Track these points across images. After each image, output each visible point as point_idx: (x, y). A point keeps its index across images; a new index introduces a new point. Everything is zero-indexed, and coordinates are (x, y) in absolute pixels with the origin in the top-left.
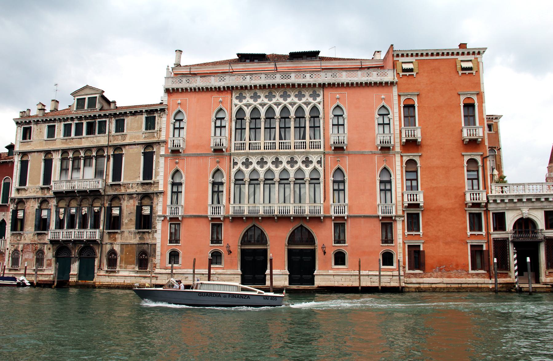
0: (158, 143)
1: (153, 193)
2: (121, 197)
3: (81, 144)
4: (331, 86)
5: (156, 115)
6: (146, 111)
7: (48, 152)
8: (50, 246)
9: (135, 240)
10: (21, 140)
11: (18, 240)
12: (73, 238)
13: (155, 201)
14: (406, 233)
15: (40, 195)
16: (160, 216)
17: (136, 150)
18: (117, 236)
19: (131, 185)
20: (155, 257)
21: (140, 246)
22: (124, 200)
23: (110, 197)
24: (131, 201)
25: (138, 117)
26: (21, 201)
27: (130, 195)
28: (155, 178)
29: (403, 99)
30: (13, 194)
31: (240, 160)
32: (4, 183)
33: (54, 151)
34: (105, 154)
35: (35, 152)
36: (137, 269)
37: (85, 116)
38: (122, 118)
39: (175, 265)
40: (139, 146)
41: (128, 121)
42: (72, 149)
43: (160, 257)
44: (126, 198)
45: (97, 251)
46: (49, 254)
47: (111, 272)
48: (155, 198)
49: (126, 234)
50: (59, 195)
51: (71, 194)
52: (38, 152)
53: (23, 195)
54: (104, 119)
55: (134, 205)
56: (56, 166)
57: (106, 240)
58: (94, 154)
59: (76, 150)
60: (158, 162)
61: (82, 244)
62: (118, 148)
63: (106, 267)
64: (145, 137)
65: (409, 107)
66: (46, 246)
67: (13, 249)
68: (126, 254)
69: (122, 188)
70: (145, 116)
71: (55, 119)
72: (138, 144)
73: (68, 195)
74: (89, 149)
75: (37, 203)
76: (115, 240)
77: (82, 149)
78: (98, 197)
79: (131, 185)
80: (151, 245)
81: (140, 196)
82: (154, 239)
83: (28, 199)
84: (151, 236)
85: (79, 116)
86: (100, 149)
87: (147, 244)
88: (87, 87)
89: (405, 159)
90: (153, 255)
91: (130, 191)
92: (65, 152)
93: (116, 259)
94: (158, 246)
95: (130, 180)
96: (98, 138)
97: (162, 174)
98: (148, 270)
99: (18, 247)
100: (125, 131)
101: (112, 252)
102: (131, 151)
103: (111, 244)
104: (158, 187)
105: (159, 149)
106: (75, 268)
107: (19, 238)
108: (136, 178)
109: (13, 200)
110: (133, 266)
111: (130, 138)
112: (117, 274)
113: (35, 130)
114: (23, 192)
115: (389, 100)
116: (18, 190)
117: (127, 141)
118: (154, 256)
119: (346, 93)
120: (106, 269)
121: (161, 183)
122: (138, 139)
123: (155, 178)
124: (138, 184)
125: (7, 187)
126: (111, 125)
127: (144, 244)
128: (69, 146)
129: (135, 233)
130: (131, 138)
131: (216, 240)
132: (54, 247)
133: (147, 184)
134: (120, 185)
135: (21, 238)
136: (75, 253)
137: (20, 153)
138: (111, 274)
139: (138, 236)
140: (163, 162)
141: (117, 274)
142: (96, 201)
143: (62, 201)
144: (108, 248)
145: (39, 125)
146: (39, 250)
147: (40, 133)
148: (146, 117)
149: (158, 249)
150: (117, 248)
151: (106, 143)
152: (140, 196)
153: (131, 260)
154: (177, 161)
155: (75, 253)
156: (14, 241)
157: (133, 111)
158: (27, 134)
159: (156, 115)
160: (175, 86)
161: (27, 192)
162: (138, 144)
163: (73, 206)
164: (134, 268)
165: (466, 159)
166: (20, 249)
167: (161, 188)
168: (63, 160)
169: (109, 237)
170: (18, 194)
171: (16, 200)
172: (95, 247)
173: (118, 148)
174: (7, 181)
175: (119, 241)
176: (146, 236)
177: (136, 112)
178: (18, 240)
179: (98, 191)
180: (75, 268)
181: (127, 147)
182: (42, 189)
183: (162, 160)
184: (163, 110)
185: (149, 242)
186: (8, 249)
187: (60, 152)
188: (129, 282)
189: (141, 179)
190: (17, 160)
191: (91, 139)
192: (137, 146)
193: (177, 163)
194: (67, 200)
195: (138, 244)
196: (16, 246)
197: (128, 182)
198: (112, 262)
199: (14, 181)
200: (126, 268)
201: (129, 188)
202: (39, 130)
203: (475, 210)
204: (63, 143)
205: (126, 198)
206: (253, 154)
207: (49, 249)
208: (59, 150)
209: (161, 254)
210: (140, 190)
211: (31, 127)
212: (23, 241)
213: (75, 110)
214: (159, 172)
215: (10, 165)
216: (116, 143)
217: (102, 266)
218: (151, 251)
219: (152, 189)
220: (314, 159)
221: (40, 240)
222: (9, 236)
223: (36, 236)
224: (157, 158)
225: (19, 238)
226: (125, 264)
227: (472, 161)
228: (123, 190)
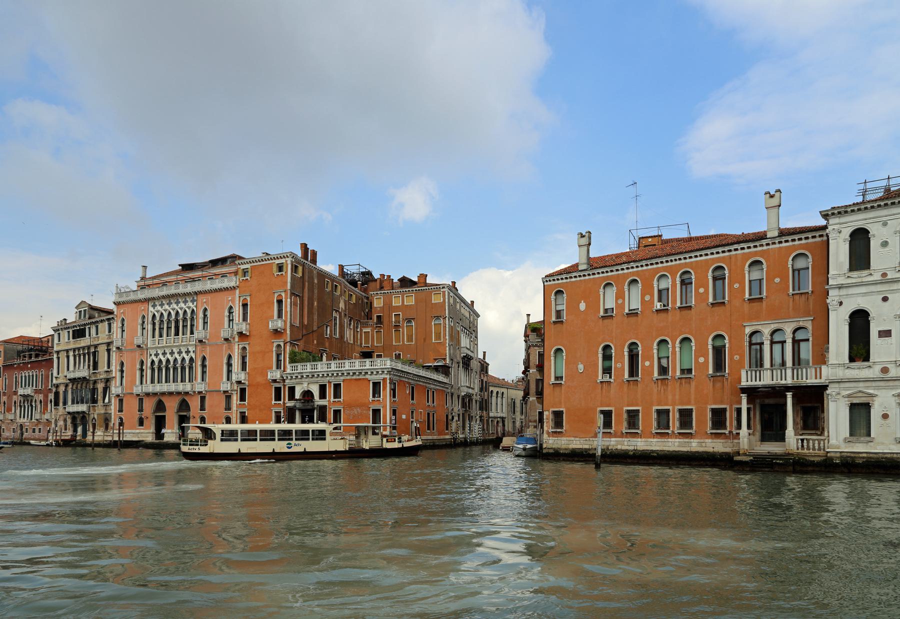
4: (200, 292)
7: (67, 351)
9: (103, 412)
14: (239, 402)
26: (57, 386)
29: (242, 299)
31: (153, 352)
46: (69, 421)
57: (92, 411)
59: (79, 349)
65: (245, 306)
74: (83, 348)
89: (241, 346)
91: (102, 377)
92: (74, 350)
106: (80, 429)
115: (233, 301)
117: (100, 342)
119: (209, 297)
131: (141, 410)
160: (120, 300)
165: (275, 345)
168: (75, 356)
173: (96, 346)
179: (84, 378)
180: (80, 429)
190: (55, 356)
203: (277, 385)
206: (159, 348)
216: (96, 343)
220: (191, 349)
227: (279, 346)
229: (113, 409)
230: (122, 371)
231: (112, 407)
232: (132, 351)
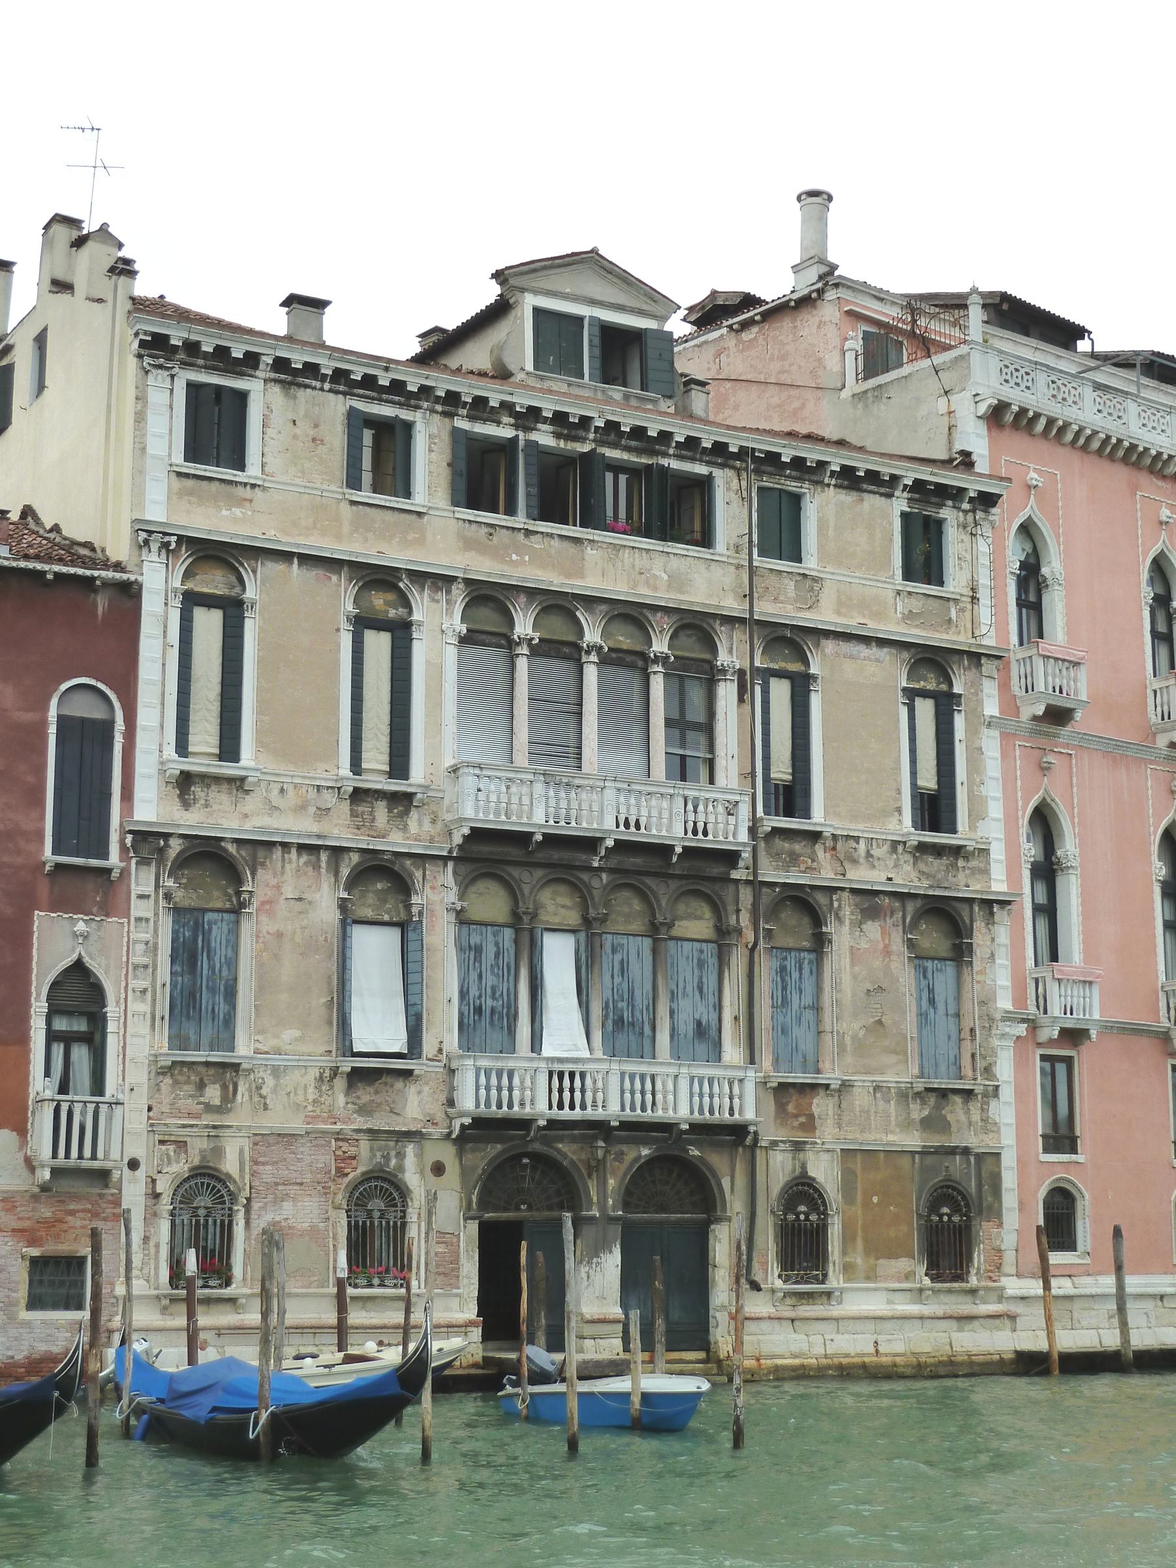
0: (975, 658)
1: (970, 901)
2: (821, 899)
3: (580, 574)
5: (947, 513)
6: (919, 486)
7: (377, 577)
8: (447, 1154)
10: (178, 457)
11: (209, 1108)
12: (614, 1108)
13: (980, 938)
15: (340, 830)
16: (1008, 1017)
17: (871, 668)
18: (820, 1105)
19: (862, 846)
20: (999, 1215)
21: (929, 1160)
22: (839, 919)
23: (767, 896)
24: (873, 929)
25: (872, 502)
27: (870, 901)
28: (972, 827)
30: (151, 805)
32: (61, 719)
33: (420, 577)
34: (723, 658)
35: (285, 556)
36: (927, 1281)
37: (612, 426)
38: (792, 486)
39: (1056, 1258)
40: (884, 653)
41: (821, 508)
42: (532, 593)
43: (1013, 1224)
44: (847, 912)
45: (726, 1183)
47: (809, 1296)
48: (979, 925)
49: (860, 1098)
50: (491, 853)
51: (556, 855)
52: (307, 560)
53: (221, 818)
54: (701, 469)
55: (887, 952)
56: (435, 671)
58: (660, 646)
60: (976, 753)
61: (645, 1142)
62: (783, 640)
63: (776, 1274)
64: (910, 616)
66: (410, 1149)
67: (180, 1168)
68: (867, 1204)
69: (819, 848)
70: (900, 504)
71: (425, 391)
72: (882, 642)
73: (540, 856)
74: (631, 614)
75: (327, 881)
76: (810, 1125)
77: (590, 601)
78: (705, 888)
79: (862, 846)
80: (980, 1157)
81: (911, 907)
82: (989, 1125)
83: (260, 847)
84: (975, 1107)
85: (575, 411)
86: (696, 626)
87: (966, 1151)
88: (590, 261)
90: (990, 1208)
92: (488, 598)
93: (825, 1227)
94: (1009, 1161)
95: (854, 817)
96: (674, 563)
97: (995, 810)
98: (973, 1281)
99: (218, 1152)
100: (811, 562)
101: (802, 1191)
102: (849, 667)
103: (798, 1147)
104: (986, 872)
105: (976, 687)
107: (213, 1094)
108: (884, 814)
109: (147, 842)
110: (903, 1264)
111: (840, 603)
112: (835, 1311)
113: (277, 420)
114: (220, 798)
116: (185, 782)
117: (825, 616)
118: (995, 1213)
120: (779, 1283)
121: (998, 852)
122: (879, 615)
123: (972, 827)
124: (894, 844)
125: (90, 752)
126: (732, 509)
127: (953, 1151)
128: (508, 570)
129: (905, 1096)
130: (842, 605)
132: (469, 1158)
133: (938, 851)
134: (815, 836)
135: (229, 1097)
136: (605, 1193)
137: (180, 538)
138: (806, 1310)
139: (918, 1111)
140: (998, 755)
141: (835, 1311)
142: (681, 908)
143: (481, 885)
144: (778, 1168)
145: (303, 395)
146: (367, 1177)
147: (291, 446)
148: (904, 515)
149: (1009, 1180)
150: (824, 1171)
151: (733, 606)
152: (911, 907)
153: (892, 1234)
154: (1050, 758)
155: (605, 1193)
156: (176, 1112)
157: (862, 465)
158: (215, 431)
159: (947, 513)
161: (251, 803)
162: (882, 642)
163: (555, 920)
164: (909, 1276)
166: (230, 1165)
167: (999, 885)
169: (781, 1108)
170: (186, 805)
171: (176, 846)
172: (718, 1161)
173: (789, 641)
174: (86, 709)
175: (828, 1134)
176: (956, 1111)
177: (873, 477)
178: (209, 1108)
181: (829, 646)
182: (359, 795)
183: (991, 743)
184: (987, 500)
185: (974, 1141)
186: (133, 1165)
187: (459, 594)
188: (899, 1347)
189: (904, 825)
191: (640, 561)
192: (874, 651)
193: (1045, 769)
194: (527, 879)
195: (925, 1152)
196: (198, 1146)
197: (855, 829)
198: (803, 1249)
199: (146, 716)
200: (871, 1276)
201: (855, 861)
202: (304, 428)
204: (469, 544)
205: (847, 912)
207: (438, 1169)
208: (450, 580)
209: (1021, 1203)
210: (906, 876)
211: (241, 397)
212: (242, 1116)
213: (530, 367)
214: (983, 801)
215: (101, 603)
217: (756, 1265)
218: (980, 1186)
219: (961, 878)
221: (364, 1110)
222: (139, 1076)
223: (340, 1083)
224: (972, 731)
225: (213, 1094)
226: (867, 1252)
228: (826, 875)
229: (1008, 1126)
230: (1047, 871)
231: (1004, 1111)
232: (1116, 752)
